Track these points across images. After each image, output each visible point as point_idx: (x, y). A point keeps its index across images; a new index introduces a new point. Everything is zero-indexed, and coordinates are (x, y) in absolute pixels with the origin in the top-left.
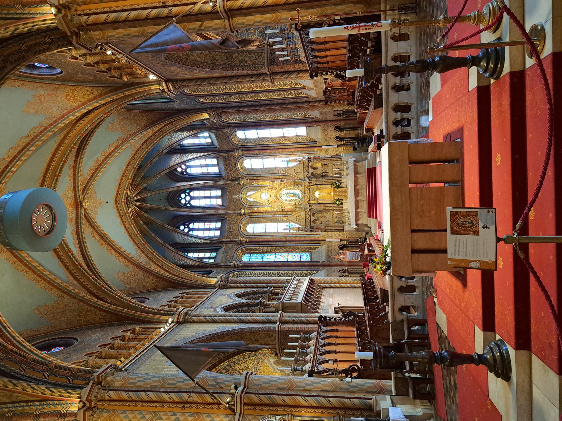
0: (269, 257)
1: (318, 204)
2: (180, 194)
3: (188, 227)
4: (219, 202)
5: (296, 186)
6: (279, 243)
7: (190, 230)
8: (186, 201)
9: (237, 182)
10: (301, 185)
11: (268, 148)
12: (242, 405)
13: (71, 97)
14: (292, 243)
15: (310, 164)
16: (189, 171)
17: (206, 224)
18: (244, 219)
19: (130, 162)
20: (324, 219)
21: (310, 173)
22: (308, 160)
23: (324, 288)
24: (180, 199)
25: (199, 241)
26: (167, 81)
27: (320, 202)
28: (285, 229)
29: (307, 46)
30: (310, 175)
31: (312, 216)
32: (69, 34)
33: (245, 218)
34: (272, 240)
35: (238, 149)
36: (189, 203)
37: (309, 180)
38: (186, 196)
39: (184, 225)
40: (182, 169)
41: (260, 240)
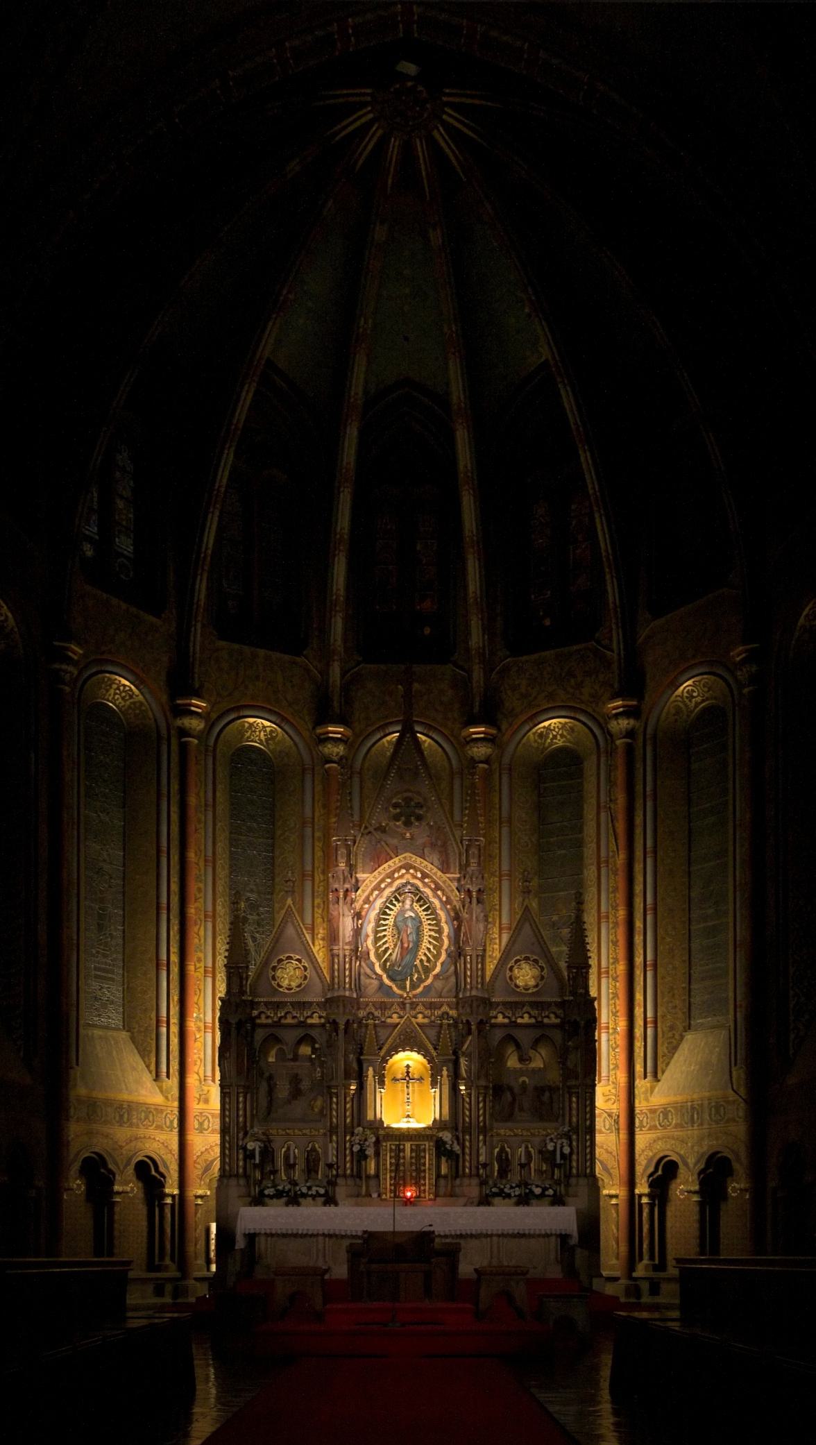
1: (360, 1063)
11: (639, 853)
14: (174, 949)
18: (297, 739)
31: (300, 1032)
41: (192, 800)
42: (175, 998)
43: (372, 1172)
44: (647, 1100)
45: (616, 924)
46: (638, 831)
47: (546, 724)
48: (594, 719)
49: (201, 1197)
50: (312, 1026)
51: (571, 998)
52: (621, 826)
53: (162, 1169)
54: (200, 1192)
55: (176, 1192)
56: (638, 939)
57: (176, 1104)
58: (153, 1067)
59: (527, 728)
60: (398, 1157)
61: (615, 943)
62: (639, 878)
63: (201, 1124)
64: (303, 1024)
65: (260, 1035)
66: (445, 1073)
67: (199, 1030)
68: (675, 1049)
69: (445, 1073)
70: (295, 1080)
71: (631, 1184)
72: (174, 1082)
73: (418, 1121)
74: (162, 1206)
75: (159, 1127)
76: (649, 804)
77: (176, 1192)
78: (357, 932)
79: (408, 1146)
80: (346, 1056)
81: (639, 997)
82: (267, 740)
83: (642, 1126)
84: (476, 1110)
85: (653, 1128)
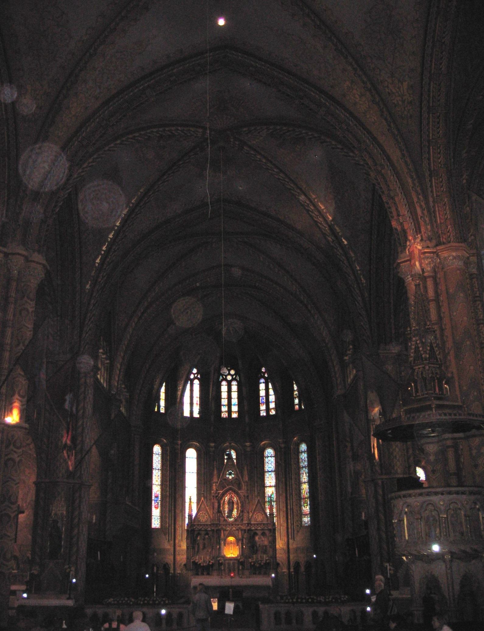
0: (156, 477)
1: (220, 540)
2: (235, 370)
4: (224, 415)
5: (241, 514)
7: (192, 381)
15: (267, 532)
16: (262, 380)
17: (198, 399)
20: (201, 547)
21: (257, 532)
24: (229, 368)
25: (179, 393)
28: (190, 499)
37: (248, 530)
38: (232, 376)
39: (197, 373)
40: (264, 373)
43: (223, 569)
49: (179, 573)
53: (169, 566)
54: (179, 572)
56: (289, 502)
57: (173, 548)
58: (167, 538)
63: (179, 553)
64: (206, 530)
65: (196, 533)
67: (178, 527)
68: (298, 532)
70: (204, 544)
71: (289, 569)
72: (172, 542)
73: (234, 555)
77: (173, 572)
79: (231, 562)
82: (195, 447)
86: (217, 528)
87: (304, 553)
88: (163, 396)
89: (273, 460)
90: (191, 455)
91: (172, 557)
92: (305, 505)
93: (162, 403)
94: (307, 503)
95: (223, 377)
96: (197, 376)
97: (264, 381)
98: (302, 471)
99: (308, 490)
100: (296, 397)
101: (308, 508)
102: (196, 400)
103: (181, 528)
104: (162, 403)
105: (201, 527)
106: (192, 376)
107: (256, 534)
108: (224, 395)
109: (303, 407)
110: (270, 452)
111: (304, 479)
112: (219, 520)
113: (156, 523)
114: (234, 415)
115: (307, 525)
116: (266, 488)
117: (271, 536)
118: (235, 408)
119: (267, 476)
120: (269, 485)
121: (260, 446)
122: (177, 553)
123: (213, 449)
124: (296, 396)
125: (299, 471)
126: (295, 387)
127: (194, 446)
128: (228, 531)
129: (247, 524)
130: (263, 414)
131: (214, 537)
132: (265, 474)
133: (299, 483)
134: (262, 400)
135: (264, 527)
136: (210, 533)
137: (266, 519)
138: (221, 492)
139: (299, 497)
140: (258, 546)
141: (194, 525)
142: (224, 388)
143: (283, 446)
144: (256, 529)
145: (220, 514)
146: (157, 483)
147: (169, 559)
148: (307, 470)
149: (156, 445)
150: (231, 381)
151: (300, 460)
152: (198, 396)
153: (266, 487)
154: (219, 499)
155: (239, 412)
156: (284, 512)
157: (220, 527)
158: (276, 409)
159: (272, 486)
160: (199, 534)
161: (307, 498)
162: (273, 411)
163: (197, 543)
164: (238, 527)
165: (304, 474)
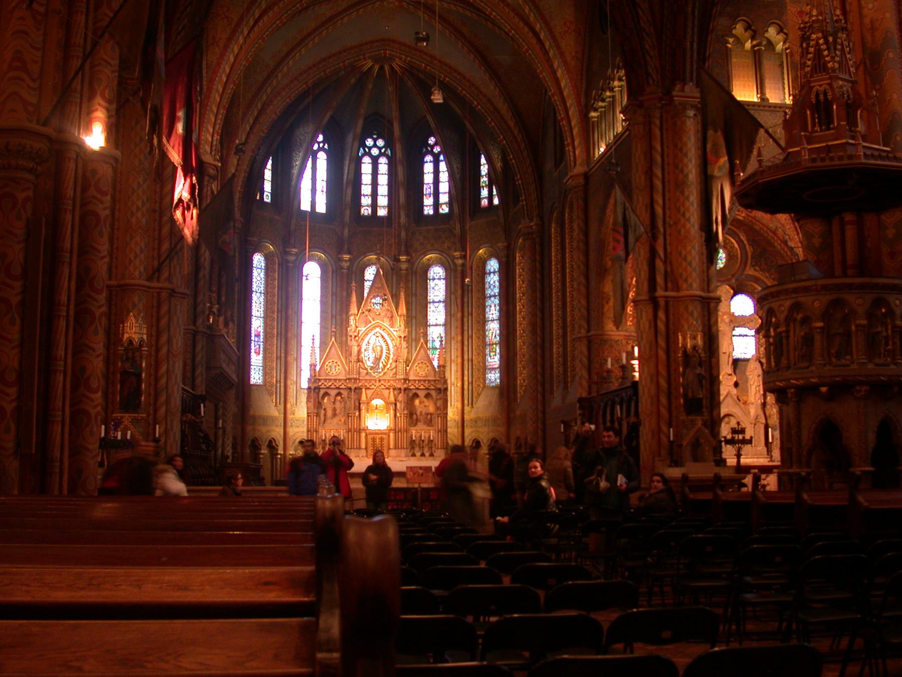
1: (360, 404)
2: (384, 139)
3: (320, 149)
4: (366, 211)
6: (283, 325)
8: (370, 148)
9: (403, 248)
10: (396, 373)
11: (466, 314)
12: (158, 290)
13: (569, 28)
14: (283, 351)
15: (433, 393)
16: (429, 158)
17: (324, 184)
18: (330, 259)
19: (455, 71)
20: (330, 413)
21: (419, 392)
22: (442, 389)
23: (216, 406)
24: (375, 136)
25: (295, 171)
26: (586, 176)
27: (363, 407)
29: (617, 396)
30: (414, 391)
31: (336, 391)
32: (641, 99)
33: (332, 263)
34: (290, 312)
35: (464, 257)
36: (365, 154)
37: (405, 389)
39: (324, 142)
40: (432, 147)
42: (283, 371)
44: (469, 415)
45: (457, 342)
46: (466, 305)
47: (430, 256)
48: (448, 256)
50: (342, 389)
51: (439, 379)
52: (459, 301)
53: (277, 443)
54: (291, 452)
55: (282, 453)
56: (466, 349)
57: (283, 415)
58: (274, 401)
59: (422, 257)
60: (374, 442)
61: (457, 350)
62: (466, 324)
65: (322, 392)
66: (391, 408)
67: (291, 384)
68: (479, 395)
69: (391, 408)
70: (334, 410)
74: (276, 458)
75: (277, 426)
76: (470, 294)
77: (282, 453)
78: (359, 352)
80: (355, 402)
81: (466, 372)
82: (318, 260)
83: (467, 426)
84: (402, 423)
85: (471, 427)
86: (355, 385)
87: (489, 427)
88: (268, 174)
89: (442, 284)
90: (312, 272)
91: (281, 431)
92: (492, 354)
93: (268, 187)
94: (495, 352)
95: (364, 150)
96: (324, 145)
97: (432, 160)
98: (488, 303)
99: (498, 332)
100: (483, 187)
101: (497, 358)
102: (321, 185)
103: (295, 386)
104: (268, 187)
105: (330, 384)
106: (316, 147)
107: (416, 395)
108: (366, 179)
109: (496, 201)
110: (437, 271)
111: (492, 314)
112: (359, 373)
113: (256, 377)
114: (382, 212)
115: (494, 384)
116: (428, 328)
117: (440, 399)
118: (383, 201)
119: (431, 310)
120: (434, 324)
121: (422, 261)
122: (289, 424)
123: (348, 264)
124: (484, 185)
125: (484, 302)
126: (484, 169)
127: (317, 258)
128: (373, 391)
129: (404, 379)
130: (428, 211)
131: (351, 399)
132: (429, 305)
133: (483, 321)
134: (428, 189)
135: (429, 384)
136: (345, 393)
137: (433, 373)
138: (364, 329)
139: (483, 343)
140: (418, 413)
141: (319, 380)
142: (366, 167)
143: (460, 262)
144: (417, 389)
145: (361, 364)
146: (258, 314)
147: (277, 433)
148: (497, 301)
149: (256, 254)
150: (378, 157)
151: (487, 286)
152: (325, 179)
153: (430, 326)
154: (360, 340)
155: (390, 206)
156: (457, 364)
157: (360, 384)
158: (450, 204)
159: (440, 325)
160: (326, 394)
161: (496, 344)
162: (444, 207)
163: (323, 407)
164: (389, 384)
165: (493, 306)
